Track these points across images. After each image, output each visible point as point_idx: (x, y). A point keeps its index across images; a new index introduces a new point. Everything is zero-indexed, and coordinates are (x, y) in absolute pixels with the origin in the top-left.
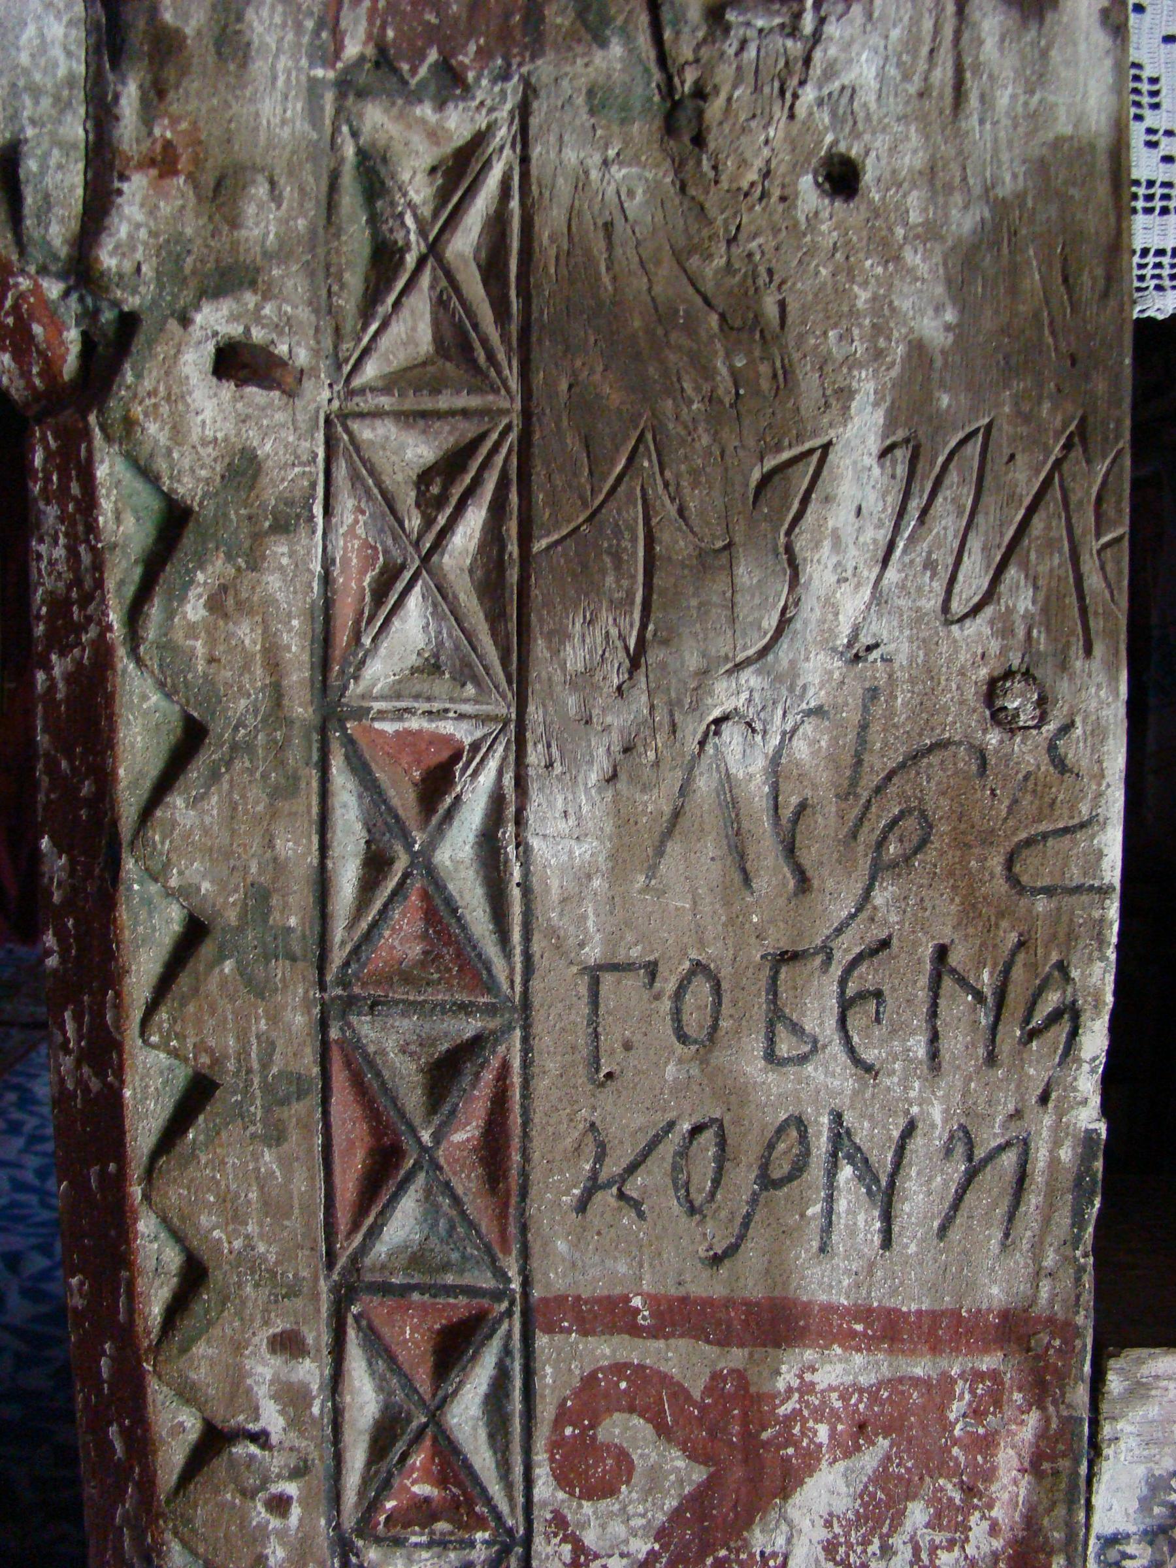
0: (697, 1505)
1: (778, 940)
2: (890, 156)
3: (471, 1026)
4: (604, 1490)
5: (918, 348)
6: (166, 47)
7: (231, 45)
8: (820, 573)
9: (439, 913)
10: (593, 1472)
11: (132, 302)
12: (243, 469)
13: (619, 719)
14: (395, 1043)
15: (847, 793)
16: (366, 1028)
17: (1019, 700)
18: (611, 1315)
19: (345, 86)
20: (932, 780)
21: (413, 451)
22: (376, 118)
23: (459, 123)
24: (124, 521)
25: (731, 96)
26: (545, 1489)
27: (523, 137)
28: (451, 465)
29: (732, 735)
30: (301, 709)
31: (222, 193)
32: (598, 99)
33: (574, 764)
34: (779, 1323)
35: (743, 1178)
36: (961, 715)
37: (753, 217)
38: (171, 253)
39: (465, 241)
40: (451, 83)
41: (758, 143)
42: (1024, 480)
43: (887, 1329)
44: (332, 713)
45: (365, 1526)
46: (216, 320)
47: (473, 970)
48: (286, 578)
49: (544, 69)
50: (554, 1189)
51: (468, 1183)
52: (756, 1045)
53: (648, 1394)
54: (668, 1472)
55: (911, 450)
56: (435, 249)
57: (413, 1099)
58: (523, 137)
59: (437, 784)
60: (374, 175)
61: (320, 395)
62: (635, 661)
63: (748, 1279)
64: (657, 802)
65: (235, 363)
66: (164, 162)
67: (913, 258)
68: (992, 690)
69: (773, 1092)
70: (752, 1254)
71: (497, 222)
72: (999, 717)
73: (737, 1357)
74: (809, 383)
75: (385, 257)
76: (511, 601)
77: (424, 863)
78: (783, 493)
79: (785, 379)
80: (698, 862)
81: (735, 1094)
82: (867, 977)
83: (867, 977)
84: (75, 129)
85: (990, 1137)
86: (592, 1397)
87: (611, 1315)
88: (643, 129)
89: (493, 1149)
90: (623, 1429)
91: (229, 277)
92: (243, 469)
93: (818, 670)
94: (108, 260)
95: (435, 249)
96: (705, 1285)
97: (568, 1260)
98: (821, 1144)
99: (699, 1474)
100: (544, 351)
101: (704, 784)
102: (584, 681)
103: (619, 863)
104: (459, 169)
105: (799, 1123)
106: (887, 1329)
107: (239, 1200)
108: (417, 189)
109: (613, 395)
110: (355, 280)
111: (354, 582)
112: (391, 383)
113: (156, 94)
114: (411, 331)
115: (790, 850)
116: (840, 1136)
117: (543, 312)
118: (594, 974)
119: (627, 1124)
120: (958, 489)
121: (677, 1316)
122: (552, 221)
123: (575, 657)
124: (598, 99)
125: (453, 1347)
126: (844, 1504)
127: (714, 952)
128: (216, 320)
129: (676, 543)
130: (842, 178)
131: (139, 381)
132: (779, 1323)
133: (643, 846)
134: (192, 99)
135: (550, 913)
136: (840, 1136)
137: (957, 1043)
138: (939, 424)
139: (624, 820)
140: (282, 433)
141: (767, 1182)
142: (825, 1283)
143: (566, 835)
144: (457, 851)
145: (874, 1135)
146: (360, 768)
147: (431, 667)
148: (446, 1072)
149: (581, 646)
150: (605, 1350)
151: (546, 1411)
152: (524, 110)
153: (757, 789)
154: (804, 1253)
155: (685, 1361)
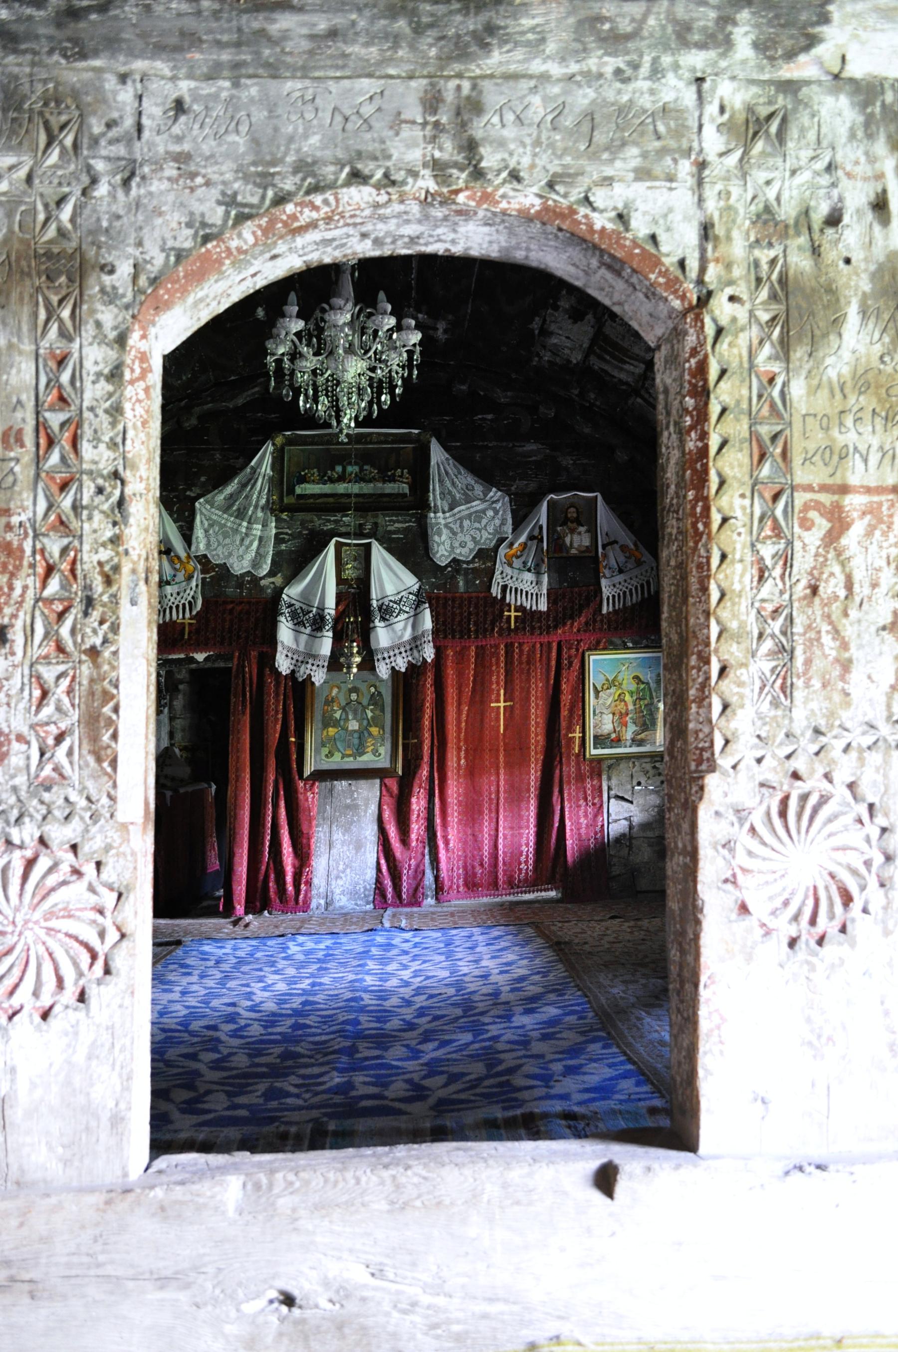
0: (829, 532)
1: (840, 408)
2: (857, 257)
3: (779, 428)
4: (808, 529)
5: (864, 294)
6: (716, 238)
7: (729, 238)
8: (846, 336)
9: (773, 405)
10: (806, 524)
11: (711, 287)
12: (734, 320)
13: (807, 367)
14: (765, 430)
15: (853, 378)
16: (759, 427)
17: (887, 359)
18: (809, 488)
19: (751, 247)
20: (870, 376)
21: (765, 317)
22: (757, 253)
23: (772, 253)
24: (710, 329)
25: (825, 247)
26: (797, 529)
27: (785, 256)
28: (773, 319)
29: (829, 369)
30: (746, 365)
31: (729, 266)
32: (800, 248)
33: (799, 374)
34: (844, 489)
35: (836, 458)
36: (875, 363)
37: (830, 269)
38: (719, 278)
39: (775, 276)
40: (770, 245)
41: (831, 255)
42: (886, 316)
43: (868, 490)
44: (752, 366)
45: (758, 540)
46: (729, 291)
47: (779, 416)
48: (743, 340)
49: (789, 242)
50: (797, 460)
51: (779, 460)
52: (836, 430)
53: (817, 506)
54: (822, 525)
55: (864, 312)
56: (769, 278)
57: (768, 442)
58: (785, 256)
59: (771, 380)
60: (757, 264)
61: (748, 306)
62: (810, 355)
63: (838, 480)
64: (815, 382)
65: (732, 299)
66: (717, 260)
67: (863, 276)
68: (881, 357)
69: (841, 439)
70: (838, 474)
71: (781, 273)
72: (883, 362)
73: (836, 497)
74: (842, 300)
75: (759, 280)
76: (785, 347)
77: (770, 395)
78: (837, 323)
79: (838, 300)
80: (824, 393)
81: (833, 440)
82: (859, 415)
83: (859, 415)
84: (697, 255)
85: (887, 447)
86: (806, 507)
87: (809, 488)
88: (808, 254)
89: (784, 454)
90: (813, 514)
91: (731, 283)
92: (734, 320)
93: (846, 355)
94: (707, 278)
95: (769, 278)
96: (830, 481)
97: (801, 476)
98: (851, 450)
99: (829, 525)
100: (791, 297)
101: (825, 378)
102: (800, 359)
103: (809, 394)
104: (773, 262)
105: (846, 446)
106: (868, 490)
107: (731, 465)
108: (765, 267)
109: (804, 305)
110: (753, 284)
111: (755, 342)
112: (762, 303)
113: (715, 248)
114: (764, 294)
115: (842, 390)
116: (855, 448)
117: (790, 289)
118: (804, 416)
119: (812, 446)
120: (873, 320)
121: (824, 488)
122: (791, 272)
123: (798, 354)
124: (800, 248)
125: (776, 497)
126: (862, 532)
127: (828, 411)
128: (729, 291)
129: (817, 332)
130: (848, 261)
131: (714, 303)
132: (844, 489)
133: (813, 391)
134: (722, 249)
135: (795, 404)
136: (855, 448)
137: (879, 427)
138: (869, 307)
139: (809, 386)
140: (741, 312)
141: (841, 458)
142: (854, 480)
143: (798, 389)
144: (776, 393)
145: (862, 448)
146: (757, 376)
147: (770, 358)
148: (774, 438)
149: (799, 353)
150: (808, 496)
151: (796, 510)
152: (785, 251)
153: (835, 379)
154: (849, 474)
155: (826, 499)
